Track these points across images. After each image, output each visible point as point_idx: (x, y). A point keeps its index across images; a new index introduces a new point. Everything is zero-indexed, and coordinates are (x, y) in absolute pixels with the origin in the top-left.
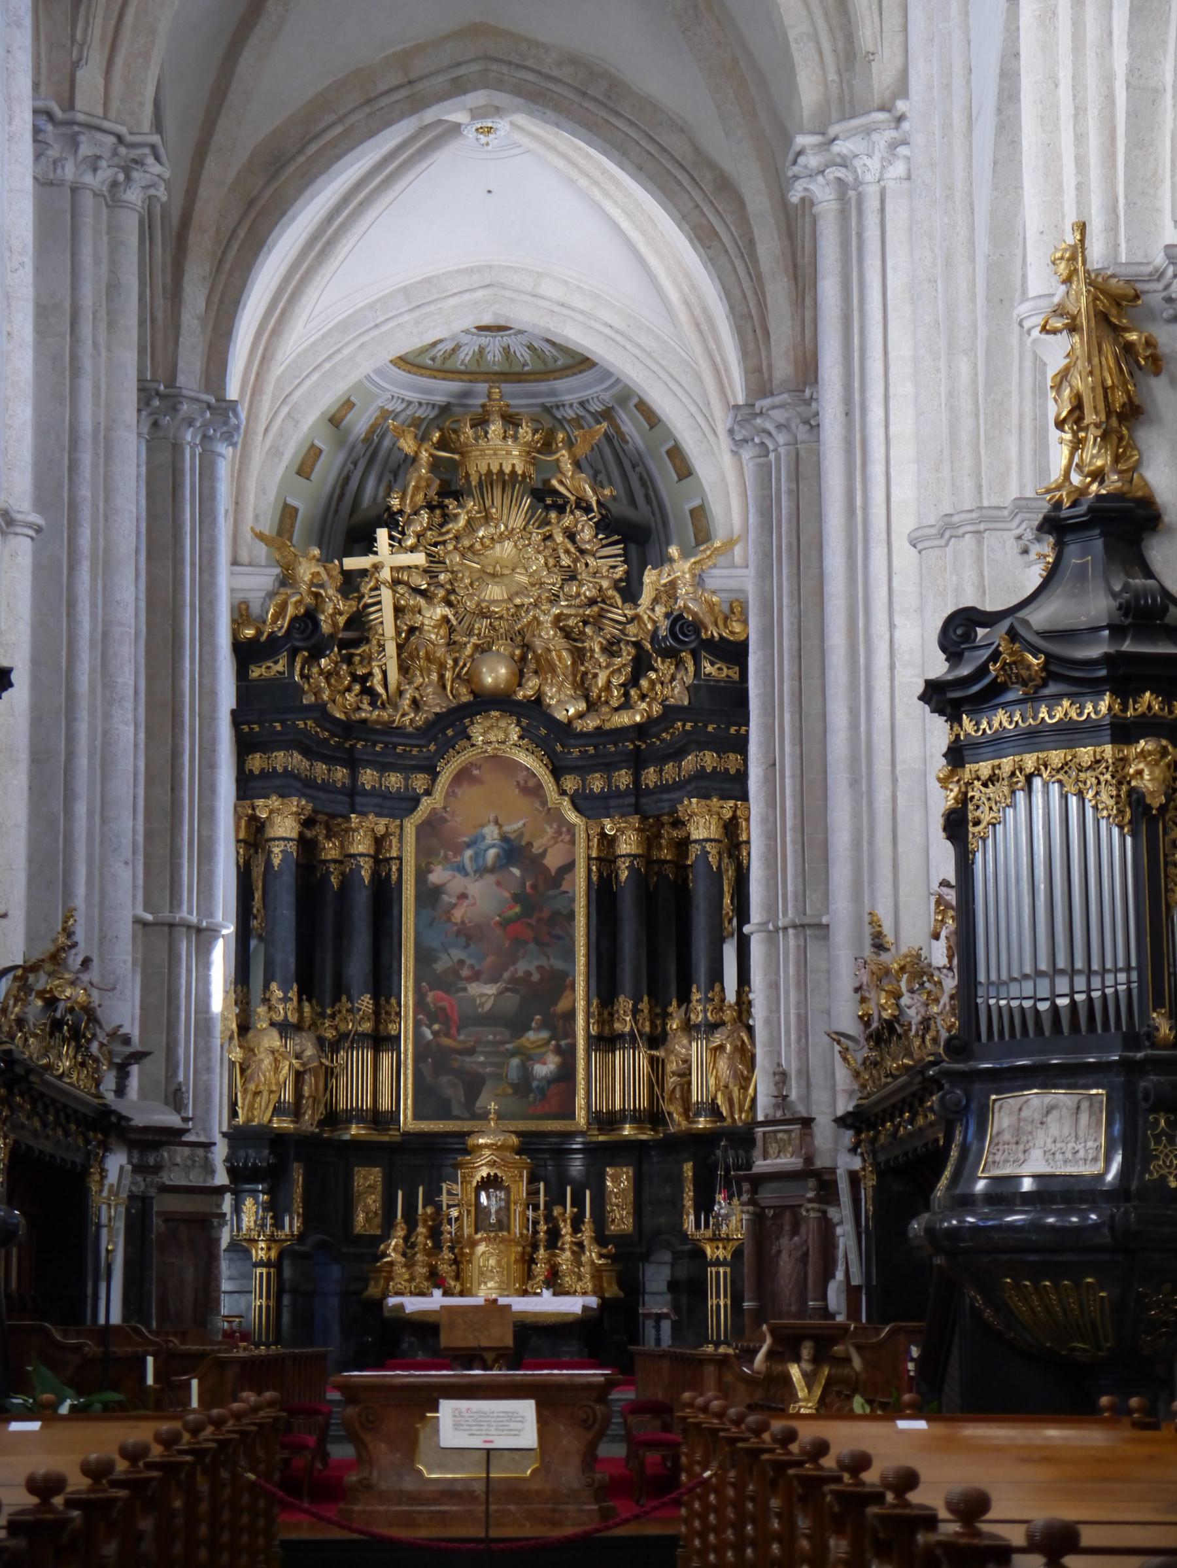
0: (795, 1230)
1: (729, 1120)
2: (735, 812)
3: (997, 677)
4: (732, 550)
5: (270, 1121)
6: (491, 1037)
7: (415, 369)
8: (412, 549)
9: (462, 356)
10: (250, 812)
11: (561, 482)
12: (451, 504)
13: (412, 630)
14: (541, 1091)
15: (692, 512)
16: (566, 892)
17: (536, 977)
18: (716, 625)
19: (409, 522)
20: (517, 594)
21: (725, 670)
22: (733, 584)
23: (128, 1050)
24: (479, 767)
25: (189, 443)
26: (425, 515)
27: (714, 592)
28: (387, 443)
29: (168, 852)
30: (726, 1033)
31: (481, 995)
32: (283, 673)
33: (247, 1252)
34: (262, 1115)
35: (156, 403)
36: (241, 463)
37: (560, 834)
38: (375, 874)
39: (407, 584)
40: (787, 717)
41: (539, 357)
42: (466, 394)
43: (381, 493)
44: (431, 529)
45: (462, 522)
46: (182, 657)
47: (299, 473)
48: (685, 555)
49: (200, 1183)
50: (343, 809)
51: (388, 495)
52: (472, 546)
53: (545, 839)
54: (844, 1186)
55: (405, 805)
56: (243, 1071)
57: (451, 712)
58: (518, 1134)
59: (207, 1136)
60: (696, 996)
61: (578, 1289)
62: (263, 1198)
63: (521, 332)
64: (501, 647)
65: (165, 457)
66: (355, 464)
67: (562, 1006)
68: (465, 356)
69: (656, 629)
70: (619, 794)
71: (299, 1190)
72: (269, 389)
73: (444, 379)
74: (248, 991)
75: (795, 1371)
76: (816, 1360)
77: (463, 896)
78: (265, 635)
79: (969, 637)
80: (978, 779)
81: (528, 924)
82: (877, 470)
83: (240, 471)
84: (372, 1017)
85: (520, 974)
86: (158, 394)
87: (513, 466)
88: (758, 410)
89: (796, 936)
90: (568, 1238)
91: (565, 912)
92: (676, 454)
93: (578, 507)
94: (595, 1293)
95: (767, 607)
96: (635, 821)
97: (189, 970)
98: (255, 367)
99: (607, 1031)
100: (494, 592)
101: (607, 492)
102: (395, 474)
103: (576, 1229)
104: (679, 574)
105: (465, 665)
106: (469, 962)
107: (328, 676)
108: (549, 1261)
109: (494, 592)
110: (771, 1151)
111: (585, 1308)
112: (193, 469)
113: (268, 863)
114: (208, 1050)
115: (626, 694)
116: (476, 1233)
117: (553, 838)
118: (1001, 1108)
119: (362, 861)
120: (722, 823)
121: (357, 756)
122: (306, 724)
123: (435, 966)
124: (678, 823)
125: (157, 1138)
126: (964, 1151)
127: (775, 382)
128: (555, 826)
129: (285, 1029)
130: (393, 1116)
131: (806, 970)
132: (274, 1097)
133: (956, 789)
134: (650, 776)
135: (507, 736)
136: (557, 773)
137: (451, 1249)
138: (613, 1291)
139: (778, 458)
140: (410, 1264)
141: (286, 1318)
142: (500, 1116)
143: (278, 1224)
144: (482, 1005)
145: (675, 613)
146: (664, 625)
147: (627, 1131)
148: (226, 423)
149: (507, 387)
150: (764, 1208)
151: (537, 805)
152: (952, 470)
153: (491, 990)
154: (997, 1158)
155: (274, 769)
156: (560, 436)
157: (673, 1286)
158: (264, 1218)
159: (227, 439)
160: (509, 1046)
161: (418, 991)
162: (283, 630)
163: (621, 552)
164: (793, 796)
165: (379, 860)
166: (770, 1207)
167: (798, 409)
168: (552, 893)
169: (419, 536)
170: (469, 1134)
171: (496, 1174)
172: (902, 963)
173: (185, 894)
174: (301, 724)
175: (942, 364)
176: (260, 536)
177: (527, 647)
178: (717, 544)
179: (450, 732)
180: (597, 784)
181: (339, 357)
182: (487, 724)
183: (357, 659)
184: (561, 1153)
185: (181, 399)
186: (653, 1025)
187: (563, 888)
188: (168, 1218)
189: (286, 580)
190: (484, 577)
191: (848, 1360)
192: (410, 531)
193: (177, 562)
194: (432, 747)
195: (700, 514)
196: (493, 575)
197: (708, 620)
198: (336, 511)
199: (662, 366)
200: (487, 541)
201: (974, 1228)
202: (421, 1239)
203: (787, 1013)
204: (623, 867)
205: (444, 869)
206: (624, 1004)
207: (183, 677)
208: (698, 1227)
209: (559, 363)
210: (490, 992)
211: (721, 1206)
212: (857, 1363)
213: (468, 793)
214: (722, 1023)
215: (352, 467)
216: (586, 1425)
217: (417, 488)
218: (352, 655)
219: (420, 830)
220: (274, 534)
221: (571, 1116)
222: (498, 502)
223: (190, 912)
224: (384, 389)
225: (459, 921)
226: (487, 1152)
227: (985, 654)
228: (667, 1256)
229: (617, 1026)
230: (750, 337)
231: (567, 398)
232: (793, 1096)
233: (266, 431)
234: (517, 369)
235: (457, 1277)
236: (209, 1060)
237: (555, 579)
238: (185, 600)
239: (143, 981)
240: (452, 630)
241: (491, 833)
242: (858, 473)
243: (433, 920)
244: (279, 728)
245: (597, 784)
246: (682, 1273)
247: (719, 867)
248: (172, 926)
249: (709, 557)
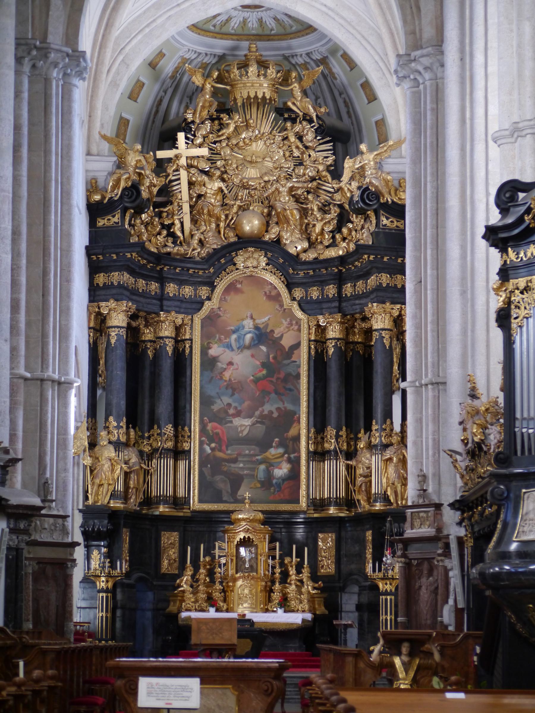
0: (430, 573)
1: (395, 505)
2: (400, 312)
3: (530, 224)
4: (401, 147)
5: (109, 503)
6: (247, 452)
7: (203, 33)
8: (200, 146)
9: (232, 24)
10: (97, 310)
11: (294, 104)
12: (225, 117)
13: (199, 196)
14: (279, 485)
15: (376, 123)
16: (295, 362)
17: (275, 415)
18: (390, 194)
19: (198, 129)
20: (266, 174)
21: (395, 222)
22: (400, 168)
23: (8, 457)
24: (241, 283)
25: (55, 78)
26: (208, 124)
27: (388, 173)
28: (185, 79)
29: (40, 334)
30: (394, 450)
31: (242, 426)
32: (118, 223)
33: (94, 583)
34: (104, 499)
35: (34, 53)
36: (93, 91)
37: (292, 325)
38: (176, 349)
39: (196, 167)
40: (429, 252)
41: (281, 25)
42: (235, 48)
43: (182, 110)
44: (212, 133)
45: (232, 128)
46: (49, 212)
47: (129, 98)
48: (371, 149)
50: (156, 309)
51: (186, 112)
52: (237, 144)
53: (282, 329)
54: (454, 546)
55: (194, 306)
56: (92, 471)
57: (223, 248)
58: (263, 512)
59: (64, 512)
60: (375, 427)
61: (300, 609)
62: (104, 550)
63: (269, 9)
64: (256, 207)
65: (40, 87)
66: (165, 92)
67: (292, 432)
68: (235, 24)
69: (352, 196)
70: (329, 301)
71: (126, 546)
72: (110, 45)
73: (221, 39)
74: (96, 422)
75: (397, 661)
76: (412, 654)
77: (230, 363)
78: (107, 199)
79: (513, 198)
80: (518, 289)
81: (272, 381)
82: (479, 95)
83: (92, 96)
84: (173, 439)
85: (266, 412)
86: (35, 47)
87: (264, 93)
88: (413, 58)
89: (433, 389)
90: (294, 577)
91: (294, 374)
92: (366, 86)
93: (304, 119)
94: (310, 611)
95: (417, 182)
96: (338, 317)
97: (53, 408)
98: (102, 31)
99: (320, 449)
100: (252, 173)
101: (323, 110)
102: (191, 99)
103: (299, 571)
104: (366, 162)
105: (232, 219)
106: (234, 405)
107: (147, 225)
108: (282, 591)
109: (252, 173)
110: (416, 524)
111: (304, 620)
112: (57, 94)
113: (109, 342)
114: (65, 458)
115: (333, 237)
116: (237, 573)
117: (288, 328)
118: (528, 497)
119: (167, 341)
120: (392, 319)
121: (165, 275)
122: (132, 255)
123: (212, 407)
124: (365, 319)
125: (25, 512)
126: (505, 525)
127: (424, 40)
128: (288, 320)
129: (118, 445)
130: (186, 501)
131: (439, 412)
132: (111, 488)
133: (504, 296)
134: (348, 289)
135: (259, 263)
136: (290, 287)
137: (221, 583)
138: (321, 610)
139: (425, 88)
140: (195, 592)
141: (118, 624)
142: (252, 501)
143: (113, 566)
144: (242, 431)
145: (364, 187)
146: (357, 194)
147: (332, 511)
148: (78, 65)
149: (260, 44)
150: (411, 559)
151: (277, 307)
152: (519, 94)
153: (247, 422)
154: (525, 529)
155: (112, 283)
156: (294, 74)
157: (359, 607)
158: (104, 563)
159: (79, 76)
160: (259, 458)
161: (201, 421)
162: (118, 196)
163: (331, 148)
164: (432, 302)
165: (178, 341)
166: (415, 559)
167: (438, 57)
168: (286, 362)
169: (204, 137)
170: (232, 512)
171: (249, 537)
172: (488, 406)
173: (51, 361)
174: (129, 255)
175: (514, 27)
176: (104, 137)
177: (271, 207)
178: (391, 143)
179: (223, 261)
180: (315, 293)
181: (154, 25)
182: (246, 255)
183: (165, 214)
184: (290, 525)
185: (50, 50)
186: (348, 444)
187: (293, 359)
188: (40, 562)
189: (120, 165)
190: (246, 163)
191: (430, 654)
192: (199, 134)
193: (47, 152)
194: (212, 270)
195: (381, 124)
196: (251, 162)
197: (384, 191)
198: (153, 122)
199: (357, 31)
200: (247, 141)
201: (509, 573)
202: (202, 577)
203: (427, 438)
204: (331, 346)
205: (219, 347)
206: (331, 431)
207: (50, 224)
208: (374, 571)
209: (294, 28)
210: (247, 424)
211: (388, 559)
212: (437, 656)
213: (233, 299)
214: (391, 444)
215: (164, 94)
216: (267, 693)
217: (203, 107)
218: (162, 212)
219: (204, 322)
220: (114, 136)
221: (297, 501)
222: (254, 116)
223: (54, 372)
224: (183, 45)
225: (228, 379)
226: (244, 523)
227: (523, 209)
228: (356, 589)
229: (326, 445)
230: (408, 11)
231: (299, 51)
232: (430, 490)
233: (109, 71)
234: (268, 32)
235: (225, 601)
236: (66, 464)
237: (290, 164)
238: (52, 176)
239: (24, 414)
240: (224, 197)
241: (248, 324)
242: (468, 97)
243: (212, 378)
244: (115, 258)
245: (315, 293)
246: (365, 599)
247: (391, 346)
248: (42, 380)
249: (385, 151)
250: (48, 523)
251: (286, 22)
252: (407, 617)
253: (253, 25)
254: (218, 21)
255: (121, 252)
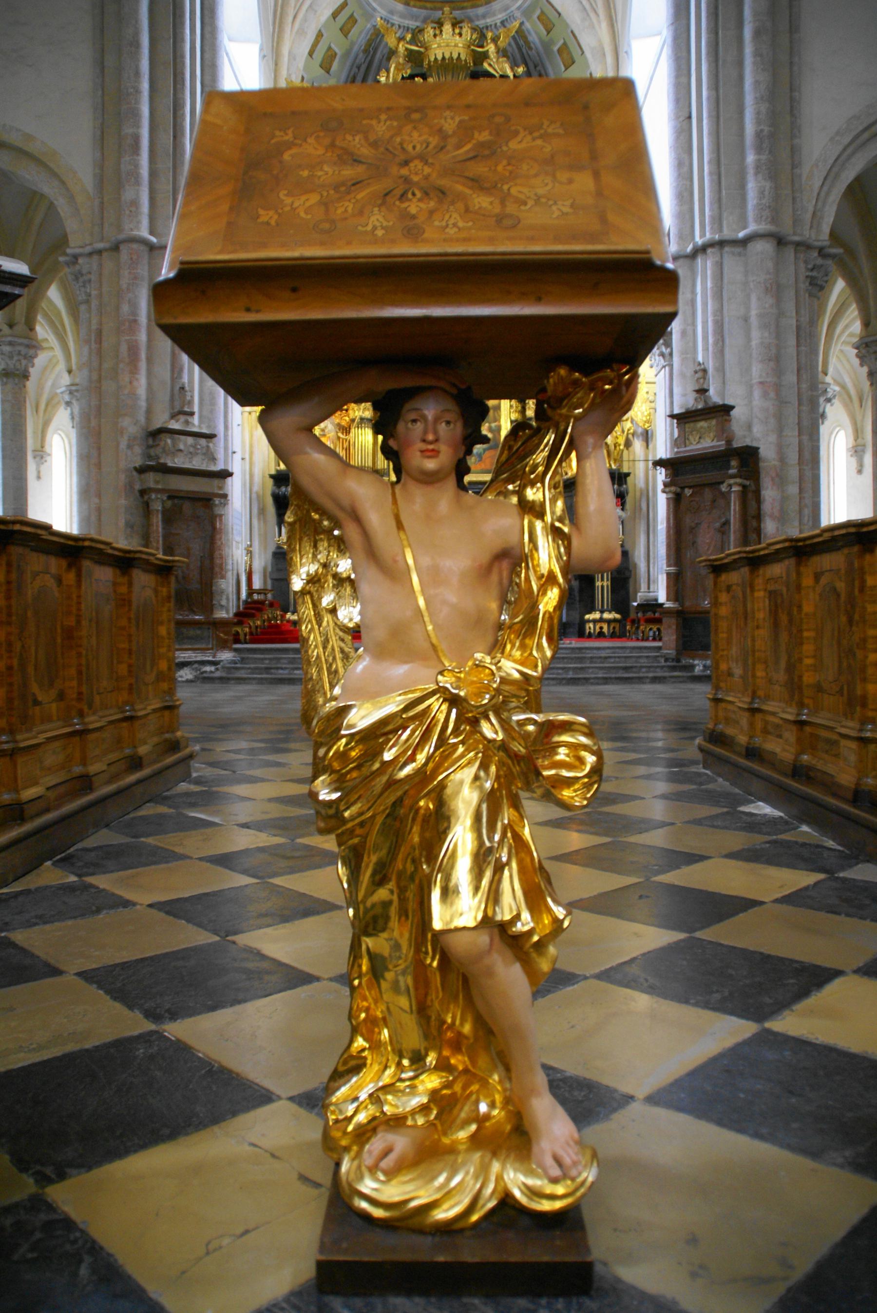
11: (490, 65)
36: (279, 37)
46: (183, 24)
49: (204, 467)
51: (378, 74)
59: (209, 427)
66: (359, 68)
87: (459, 54)
164: (710, 134)
188: (173, 496)
250: (185, 444)
252: (676, 565)
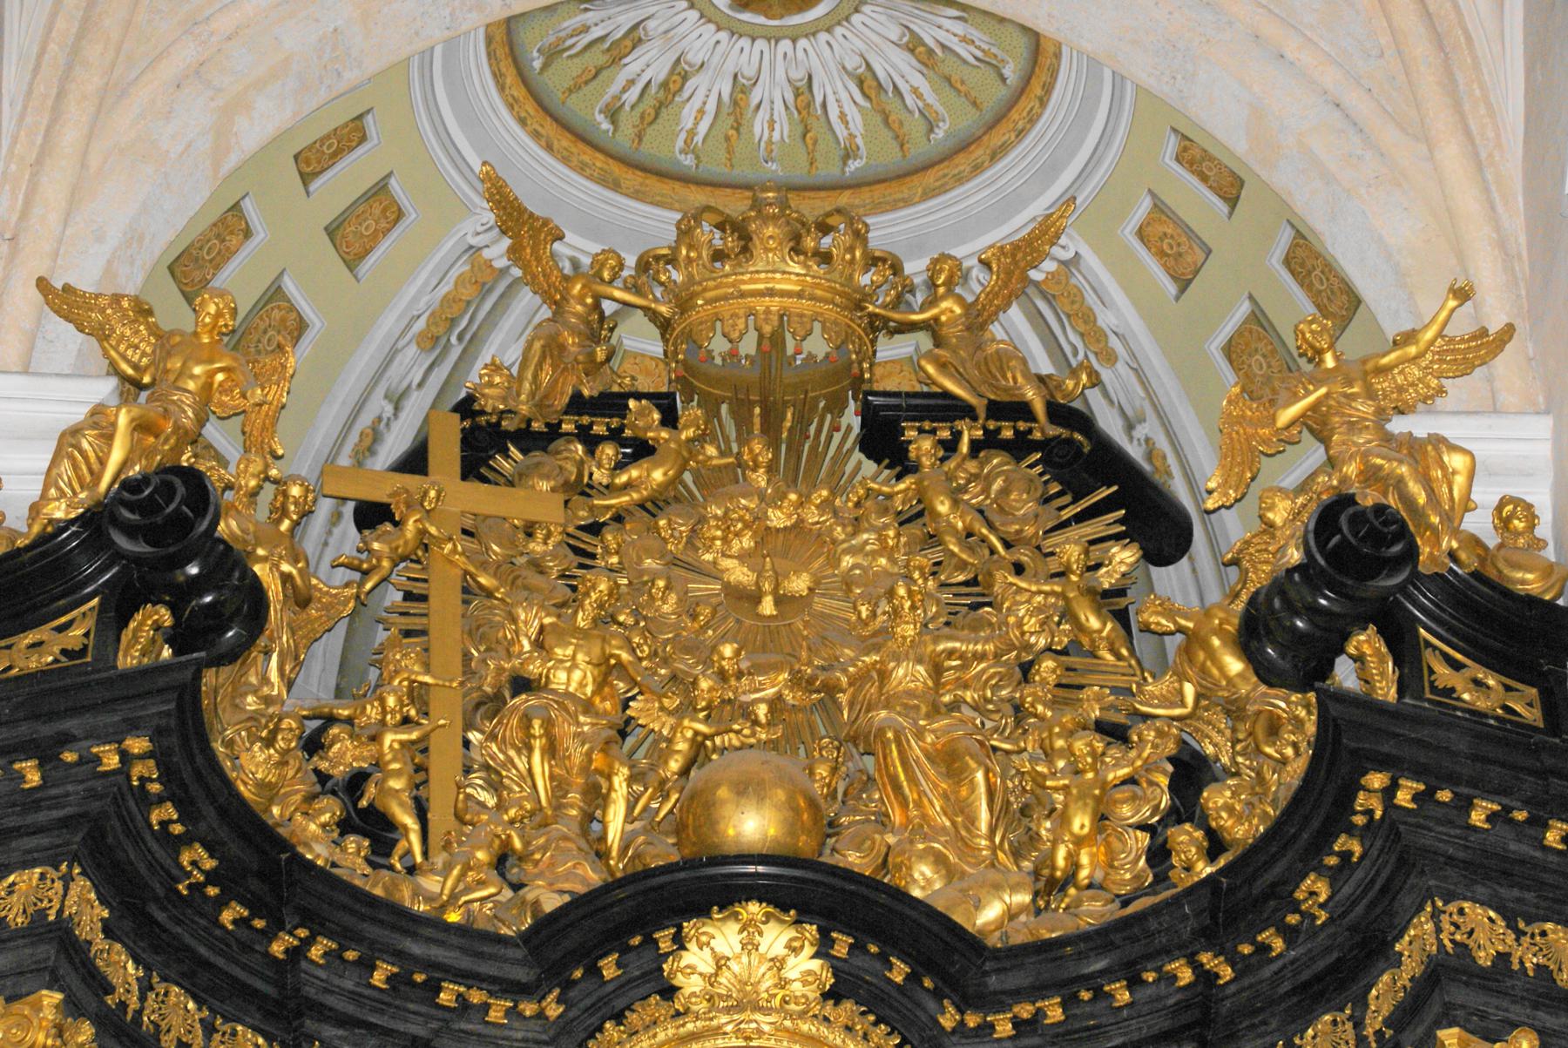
7: (564, 142)
9: (688, 116)
32: (83, 651)
73: (638, 195)
121: (310, 991)
122: (125, 756)
209: (940, 134)
244: (34, 778)
251: (910, 100)
253: (772, 122)
254: (632, 82)
255: (66, 740)
